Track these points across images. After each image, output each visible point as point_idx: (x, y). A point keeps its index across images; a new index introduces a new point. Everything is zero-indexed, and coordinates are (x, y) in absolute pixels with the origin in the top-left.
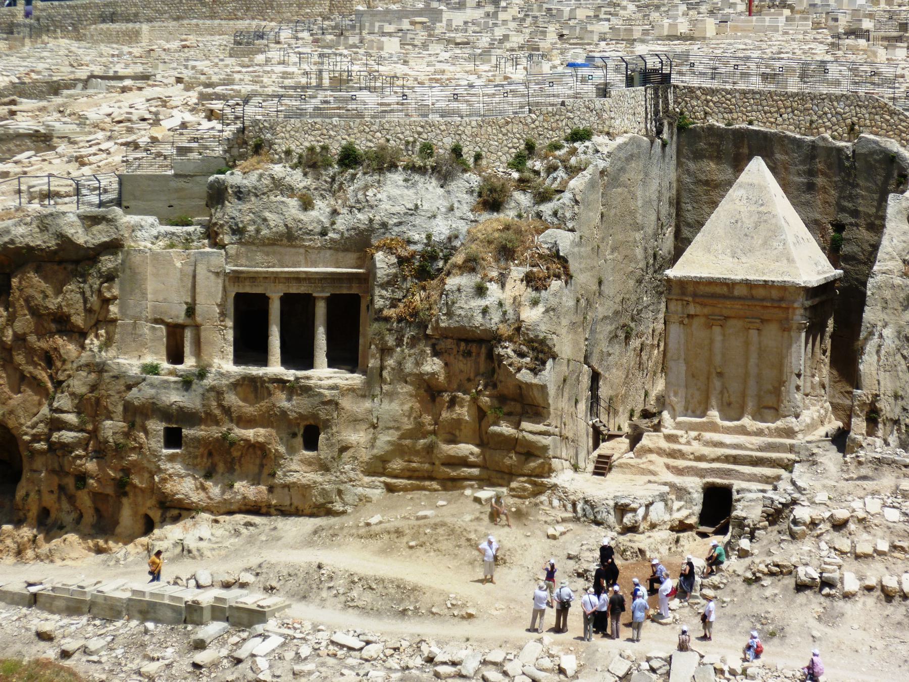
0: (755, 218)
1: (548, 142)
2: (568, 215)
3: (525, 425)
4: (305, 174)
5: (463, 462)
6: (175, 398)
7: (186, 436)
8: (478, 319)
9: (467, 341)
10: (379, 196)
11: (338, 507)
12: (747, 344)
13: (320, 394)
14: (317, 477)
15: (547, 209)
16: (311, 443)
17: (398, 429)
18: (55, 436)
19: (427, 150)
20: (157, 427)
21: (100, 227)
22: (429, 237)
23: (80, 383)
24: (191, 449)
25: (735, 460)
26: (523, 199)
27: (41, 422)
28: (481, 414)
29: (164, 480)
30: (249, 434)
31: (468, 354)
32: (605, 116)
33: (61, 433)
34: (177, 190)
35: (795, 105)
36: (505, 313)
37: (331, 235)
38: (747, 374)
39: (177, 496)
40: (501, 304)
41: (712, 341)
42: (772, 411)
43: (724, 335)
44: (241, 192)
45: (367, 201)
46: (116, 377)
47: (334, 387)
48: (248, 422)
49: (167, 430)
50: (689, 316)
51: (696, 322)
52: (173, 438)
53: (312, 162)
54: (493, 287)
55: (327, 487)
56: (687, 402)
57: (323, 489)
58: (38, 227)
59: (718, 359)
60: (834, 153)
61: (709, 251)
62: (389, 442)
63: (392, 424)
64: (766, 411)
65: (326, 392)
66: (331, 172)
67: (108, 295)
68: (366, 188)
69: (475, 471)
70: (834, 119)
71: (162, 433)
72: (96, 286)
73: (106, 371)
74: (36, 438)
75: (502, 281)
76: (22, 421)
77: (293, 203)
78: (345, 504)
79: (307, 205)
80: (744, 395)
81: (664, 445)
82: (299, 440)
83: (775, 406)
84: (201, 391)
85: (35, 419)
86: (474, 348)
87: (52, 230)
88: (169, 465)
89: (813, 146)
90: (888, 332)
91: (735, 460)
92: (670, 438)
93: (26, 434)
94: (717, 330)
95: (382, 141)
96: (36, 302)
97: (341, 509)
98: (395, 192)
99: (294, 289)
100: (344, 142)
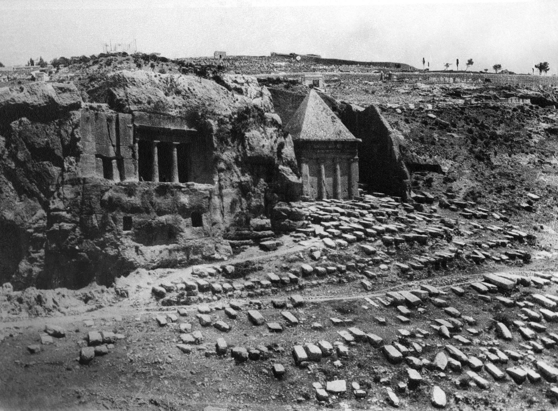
3: (293, 204)
5: (262, 228)
7: (135, 222)
11: (217, 256)
16: (197, 222)
18: (56, 227)
23: (68, 192)
27: (41, 219)
29: (123, 249)
30: (163, 218)
33: (61, 224)
39: (130, 260)
45: (191, 92)
46: (94, 186)
48: (160, 213)
49: (125, 218)
57: (209, 247)
58: (28, 92)
69: (270, 232)
71: (122, 220)
72: (70, 131)
73: (88, 183)
74: (37, 230)
76: (26, 220)
78: (221, 254)
85: (34, 218)
87: (40, 93)
93: (30, 228)
96: (32, 140)
97: (220, 258)
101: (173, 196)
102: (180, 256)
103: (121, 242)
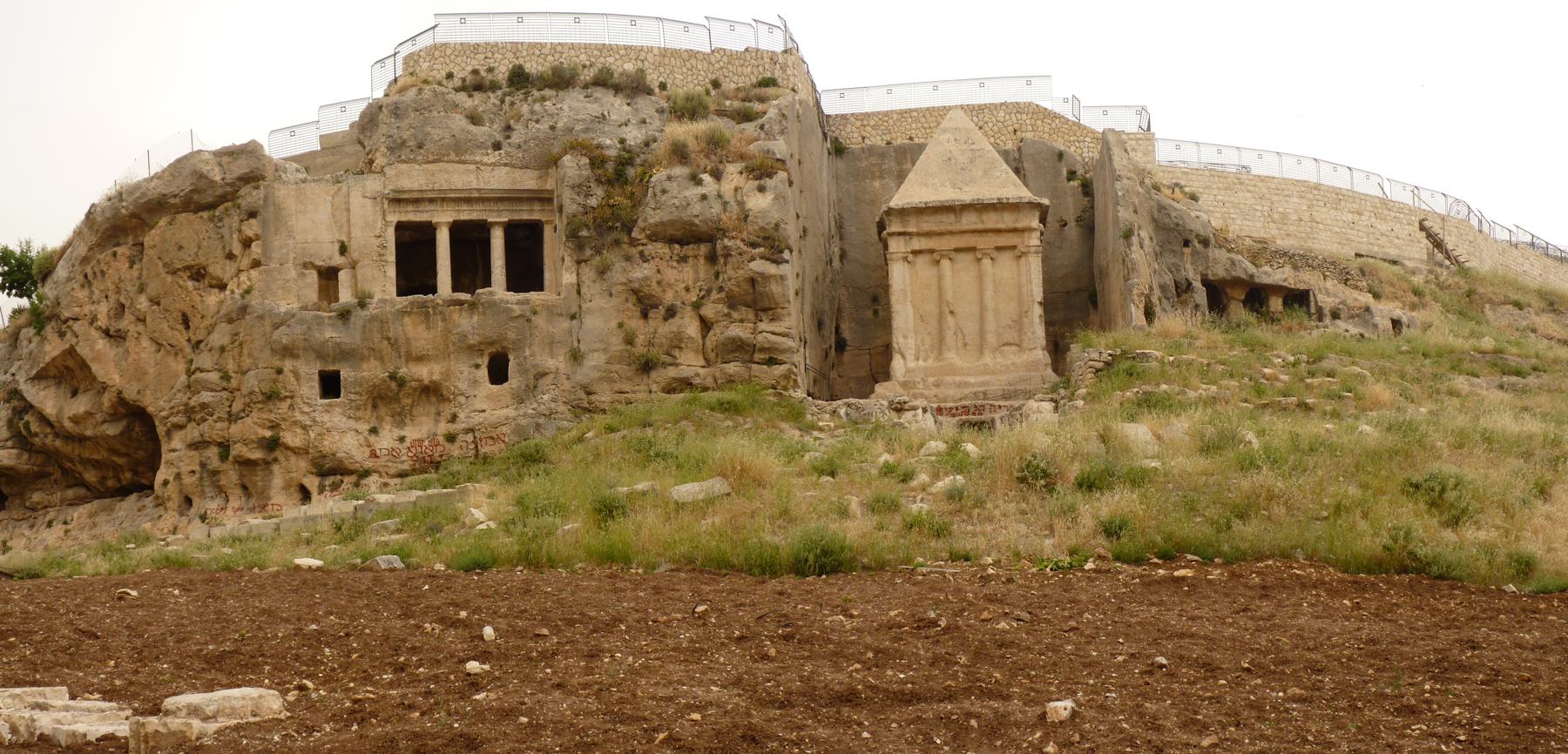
6: (330, 334)
8: (697, 208)
9: (682, 242)
17: (605, 350)
20: (310, 371)
22: (622, 141)
24: (353, 397)
28: (706, 325)
31: (683, 259)
52: (330, 385)
54: (706, 177)
62: (595, 367)
63: (596, 346)
71: (316, 377)
75: (717, 175)
82: (483, 373)
84: (361, 322)
86: (689, 250)
88: (326, 417)
101: (444, 320)
103: (314, 420)
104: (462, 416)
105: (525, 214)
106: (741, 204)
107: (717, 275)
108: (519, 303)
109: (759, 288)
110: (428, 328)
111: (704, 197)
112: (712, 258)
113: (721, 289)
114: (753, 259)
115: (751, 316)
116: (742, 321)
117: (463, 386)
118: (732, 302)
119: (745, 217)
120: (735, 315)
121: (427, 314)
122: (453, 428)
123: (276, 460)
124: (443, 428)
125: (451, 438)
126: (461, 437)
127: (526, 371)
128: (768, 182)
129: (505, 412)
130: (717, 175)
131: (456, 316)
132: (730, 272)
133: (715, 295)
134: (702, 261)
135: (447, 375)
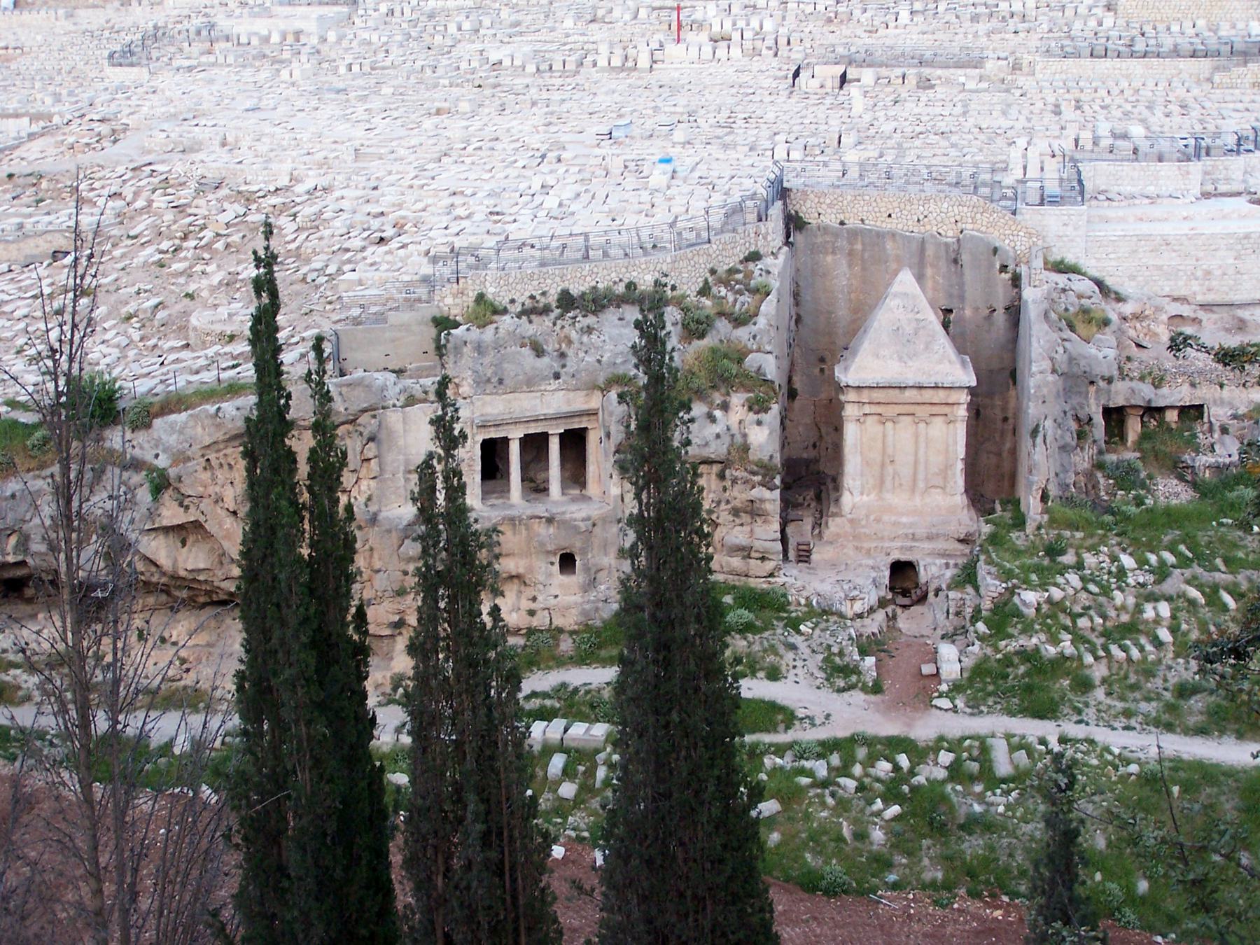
0: (914, 325)
1: (726, 267)
2: (765, 339)
4: (530, 322)
10: (602, 338)
12: (917, 436)
13: (576, 528)
14: (578, 598)
15: (742, 333)
19: (631, 286)
21: (356, 393)
25: (914, 538)
26: (723, 326)
32: (769, 238)
34: (393, 341)
35: (902, 205)
36: (733, 436)
37: (563, 377)
38: (916, 462)
40: (728, 429)
41: (884, 436)
42: (939, 490)
43: (894, 429)
44: (479, 346)
46: (389, 531)
47: (588, 519)
50: (866, 415)
51: (869, 419)
53: (533, 311)
54: (718, 413)
55: (587, 607)
56: (863, 486)
59: (890, 451)
60: (943, 248)
61: (878, 356)
64: (933, 490)
65: (581, 524)
66: (553, 316)
67: (370, 455)
68: (589, 330)
70: (939, 218)
75: (725, 407)
77: (527, 351)
79: (539, 351)
80: (915, 480)
81: (848, 528)
83: (941, 484)
89: (923, 242)
90: (1049, 423)
91: (914, 538)
92: (851, 521)
94: (889, 425)
95: (594, 283)
98: (615, 331)
99: (533, 429)
100: (559, 289)
101: (527, 529)
102: (540, 621)
104: (540, 598)
105: (575, 425)
106: (745, 436)
107: (725, 489)
108: (583, 520)
109: (756, 505)
110: (514, 534)
111: (718, 436)
112: (722, 476)
113: (728, 502)
114: (753, 487)
115: (749, 520)
116: (742, 525)
117: (541, 578)
118: (736, 512)
119: (746, 448)
120: (738, 521)
121: (514, 525)
122: (533, 606)
123: (400, 634)
124: (526, 604)
125: (532, 613)
126: (539, 613)
127: (589, 569)
128: (762, 416)
129: (573, 598)
130: (725, 407)
131: (536, 526)
132: (735, 493)
133: (723, 506)
134: (714, 477)
135: (530, 569)
